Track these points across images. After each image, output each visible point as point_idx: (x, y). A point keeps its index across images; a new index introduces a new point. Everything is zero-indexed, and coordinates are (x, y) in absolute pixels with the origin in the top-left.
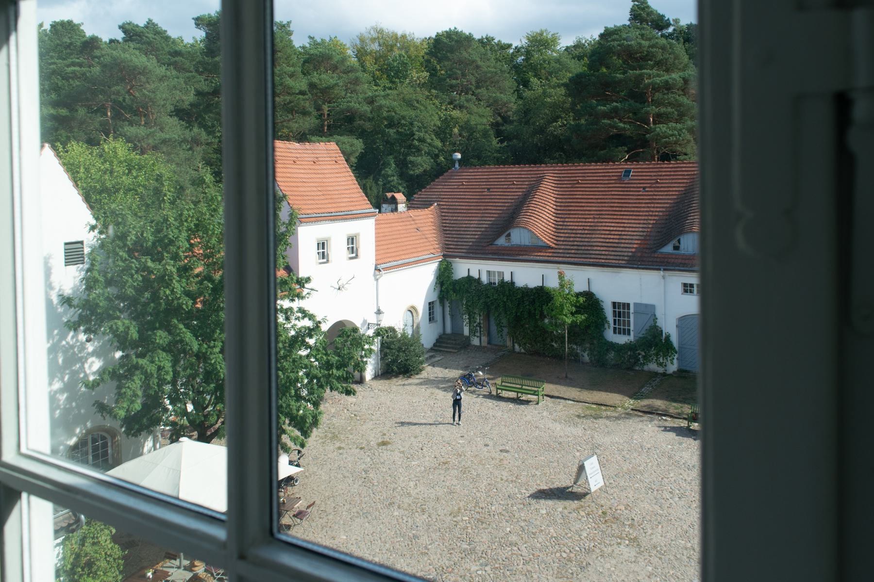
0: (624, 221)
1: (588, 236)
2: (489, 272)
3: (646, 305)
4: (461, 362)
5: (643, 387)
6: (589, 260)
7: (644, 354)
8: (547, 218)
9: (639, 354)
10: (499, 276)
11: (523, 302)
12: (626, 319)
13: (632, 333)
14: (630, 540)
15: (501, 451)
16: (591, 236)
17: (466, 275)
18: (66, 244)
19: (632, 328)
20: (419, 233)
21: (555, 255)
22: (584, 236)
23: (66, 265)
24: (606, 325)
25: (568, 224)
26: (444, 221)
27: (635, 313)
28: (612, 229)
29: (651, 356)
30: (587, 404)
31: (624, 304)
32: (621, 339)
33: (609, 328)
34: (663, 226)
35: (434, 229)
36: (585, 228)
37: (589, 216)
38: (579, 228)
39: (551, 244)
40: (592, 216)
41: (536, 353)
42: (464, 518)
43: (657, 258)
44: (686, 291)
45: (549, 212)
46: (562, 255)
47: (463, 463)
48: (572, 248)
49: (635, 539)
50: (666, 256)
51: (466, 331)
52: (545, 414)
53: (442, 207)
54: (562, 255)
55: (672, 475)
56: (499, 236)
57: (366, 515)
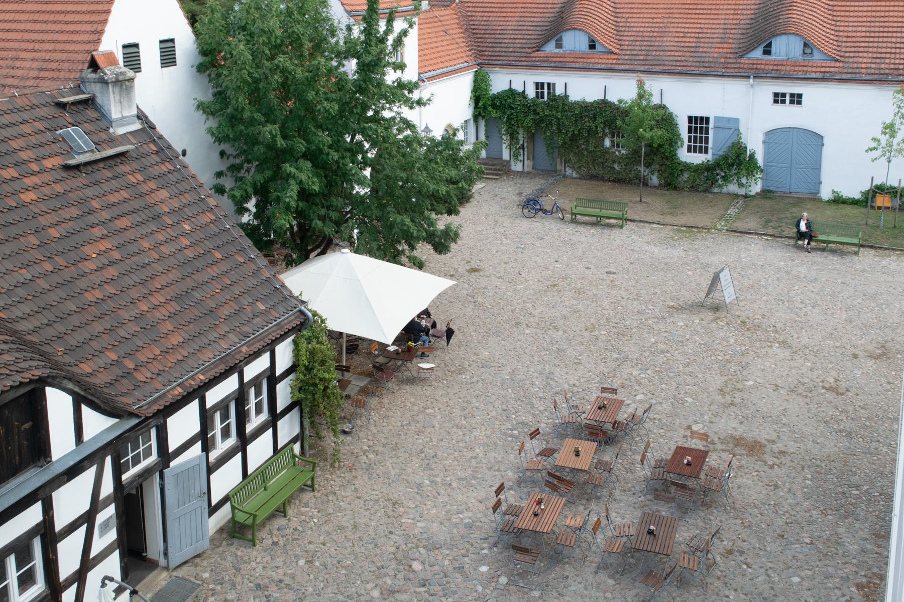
0: (700, 21)
1: (658, 39)
2: (537, 84)
3: (729, 120)
4: (510, 189)
5: (728, 209)
6: (662, 67)
7: (723, 174)
8: (605, 18)
9: (718, 174)
10: (549, 88)
11: (581, 117)
12: (704, 135)
13: (710, 151)
14: (778, 342)
15: (607, 273)
16: (661, 39)
17: (507, 87)
18: (161, 42)
19: (710, 145)
20: (448, 37)
21: (620, 62)
22: (654, 39)
23: (162, 67)
24: (679, 143)
25: (632, 25)
26: (472, 23)
27: (715, 127)
28: (686, 30)
29: (731, 176)
30: (675, 227)
31: (702, 118)
32: (697, 159)
33: (682, 147)
34: (749, 26)
35: (461, 33)
36: (653, 29)
37: (656, 16)
38: (646, 29)
39: (613, 49)
40: (660, 16)
41: (593, 177)
42: (602, 333)
43: (744, 64)
44: (776, 101)
45: (607, 10)
46: (629, 62)
47: (573, 286)
48: (640, 53)
49: (784, 342)
50: (755, 62)
51: (506, 155)
52: (634, 237)
53: (466, 5)
54: (629, 62)
55: (797, 287)
56: (546, 41)
57: (497, 334)
